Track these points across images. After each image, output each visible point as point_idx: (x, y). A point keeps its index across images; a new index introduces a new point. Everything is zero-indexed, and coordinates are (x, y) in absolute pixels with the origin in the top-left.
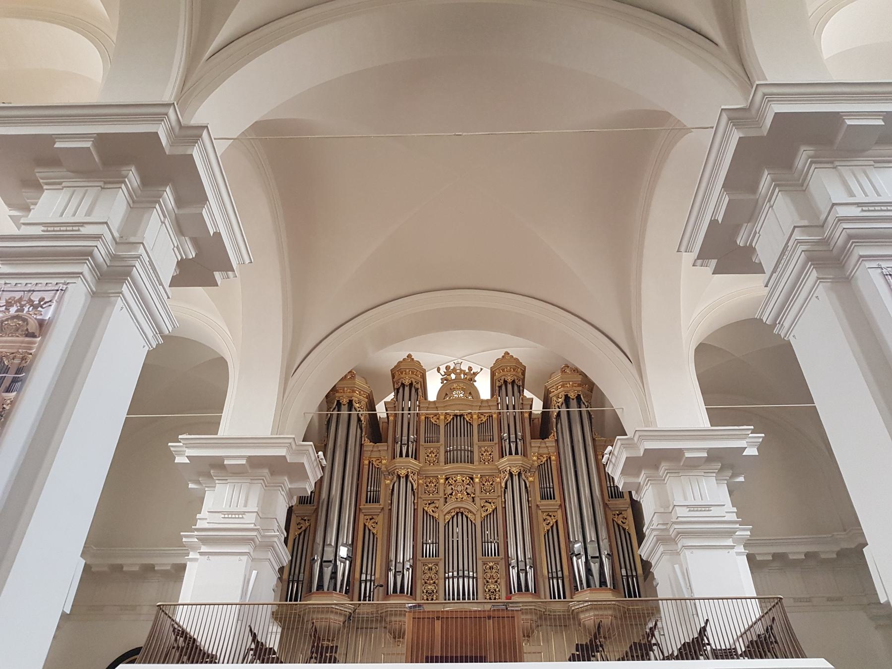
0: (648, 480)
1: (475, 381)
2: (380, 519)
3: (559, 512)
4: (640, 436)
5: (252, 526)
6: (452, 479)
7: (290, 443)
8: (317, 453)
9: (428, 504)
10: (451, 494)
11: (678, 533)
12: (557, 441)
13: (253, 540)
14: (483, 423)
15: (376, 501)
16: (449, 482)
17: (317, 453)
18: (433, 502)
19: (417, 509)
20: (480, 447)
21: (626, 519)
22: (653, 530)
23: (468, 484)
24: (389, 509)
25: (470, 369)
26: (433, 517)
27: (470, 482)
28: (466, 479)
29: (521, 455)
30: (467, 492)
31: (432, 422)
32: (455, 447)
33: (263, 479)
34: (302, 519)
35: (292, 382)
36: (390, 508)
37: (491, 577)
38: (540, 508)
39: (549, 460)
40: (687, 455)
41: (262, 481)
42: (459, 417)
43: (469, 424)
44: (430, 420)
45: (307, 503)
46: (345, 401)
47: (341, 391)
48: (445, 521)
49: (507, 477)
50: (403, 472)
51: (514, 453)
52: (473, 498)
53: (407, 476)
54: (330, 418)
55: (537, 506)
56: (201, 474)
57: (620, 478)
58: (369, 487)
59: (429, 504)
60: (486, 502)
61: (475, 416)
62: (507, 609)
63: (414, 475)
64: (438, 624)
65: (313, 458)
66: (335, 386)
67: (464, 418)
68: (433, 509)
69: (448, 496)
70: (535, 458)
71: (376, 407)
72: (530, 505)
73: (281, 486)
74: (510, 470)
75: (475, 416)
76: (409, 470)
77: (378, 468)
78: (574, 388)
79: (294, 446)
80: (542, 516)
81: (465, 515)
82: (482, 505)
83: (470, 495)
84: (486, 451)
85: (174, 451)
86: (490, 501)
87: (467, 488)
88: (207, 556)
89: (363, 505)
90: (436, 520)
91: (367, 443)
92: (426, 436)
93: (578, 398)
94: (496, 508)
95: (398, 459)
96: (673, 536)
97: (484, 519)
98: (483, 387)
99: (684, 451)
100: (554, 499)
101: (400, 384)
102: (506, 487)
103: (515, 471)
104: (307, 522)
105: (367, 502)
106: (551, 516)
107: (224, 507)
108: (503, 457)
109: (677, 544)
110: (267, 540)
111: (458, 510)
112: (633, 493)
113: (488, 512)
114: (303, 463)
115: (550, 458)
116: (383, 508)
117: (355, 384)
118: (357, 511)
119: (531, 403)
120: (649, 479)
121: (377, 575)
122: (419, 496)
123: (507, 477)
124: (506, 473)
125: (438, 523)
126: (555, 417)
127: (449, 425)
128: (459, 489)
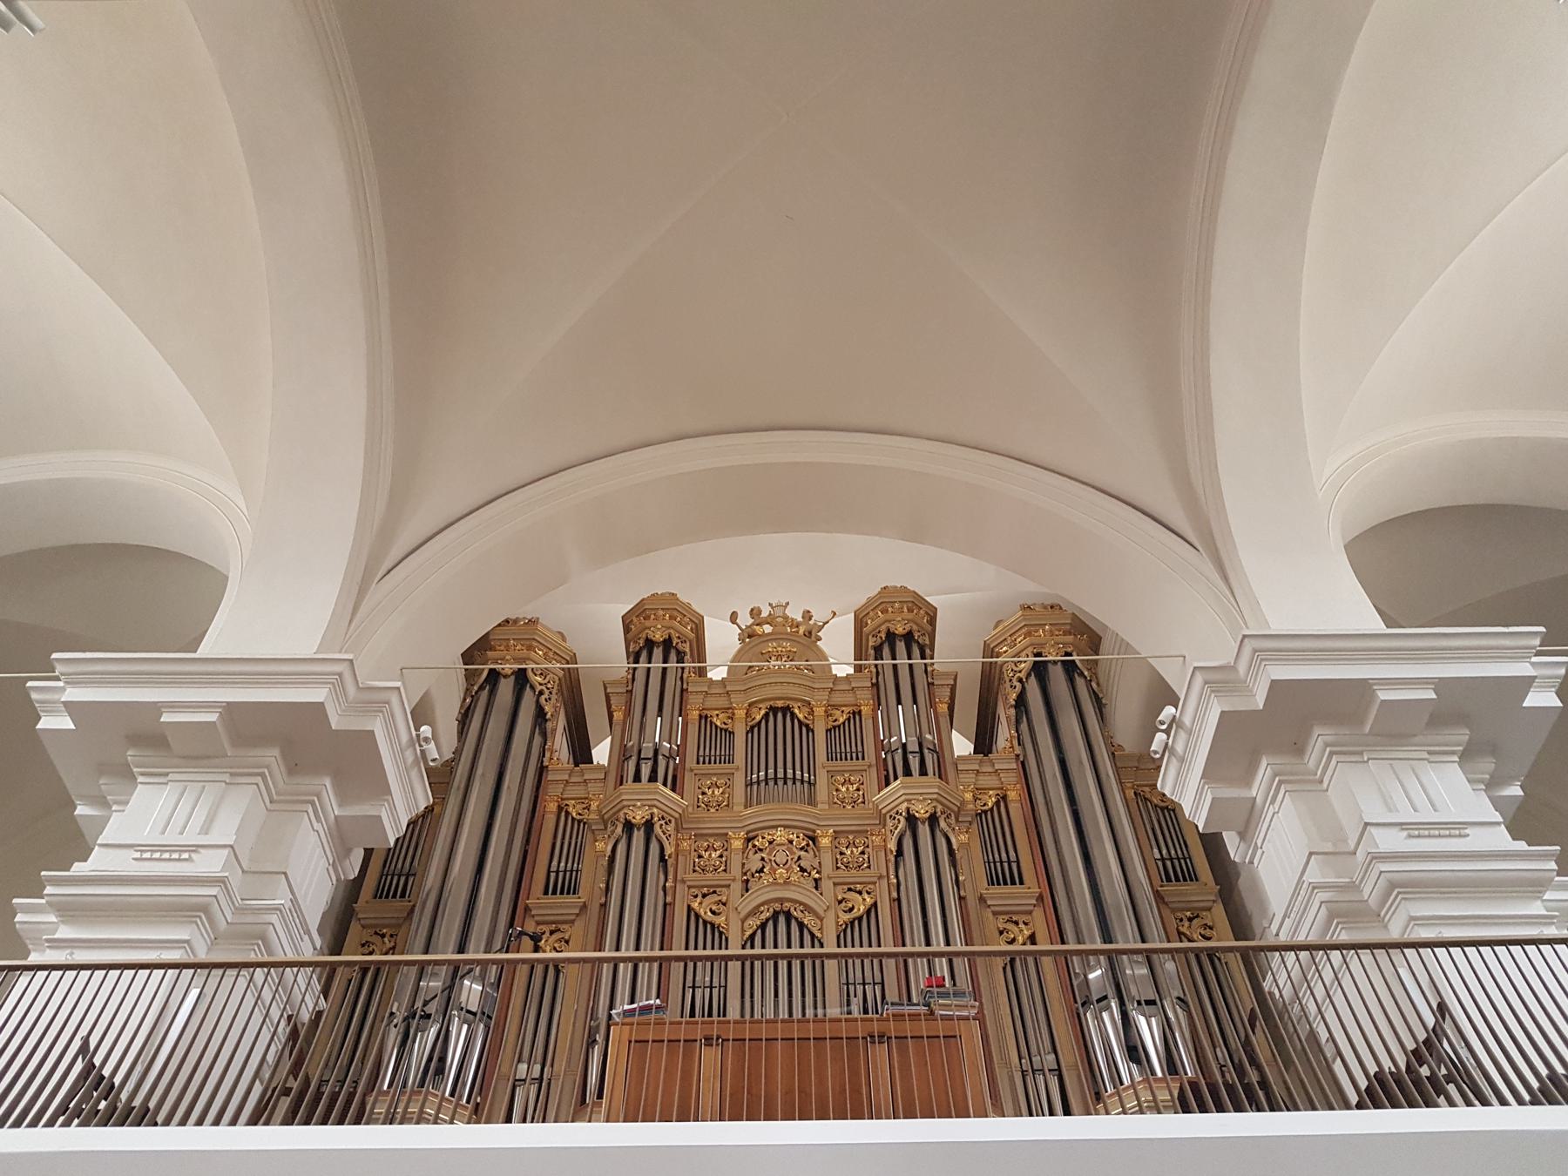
0: (1280, 782)
1: (820, 639)
4: (1255, 651)
6: (763, 838)
7: (340, 675)
8: (417, 729)
9: (700, 896)
10: (761, 871)
11: (1392, 885)
13: (205, 909)
14: (839, 726)
15: (571, 889)
16: (754, 846)
17: (417, 729)
18: (714, 892)
19: (673, 904)
21: (1211, 928)
22: (1315, 887)
23: (802, 849)
24: (601, 905)
25: (807, 615)
26: (713, 925)
27: (808, 845)
28: (798, 837)
29: (934, 775)
30: (799, 866)
31: (716, 726)
32: (771, 771)
33: (262, 775)
34: (376, 933)
35: (377, 593)
36: (603, 900)
38: (989, 903)
39: (1002, 804)
40: (1384, 695)
41: (259, 780)
42: (780, 715)
43: (804, 729)
44: (711, 722)
45: (394, 896)
47: (502, 648)
48: (743, 931)
49: (900, 826)
50: (639, 816)
52: (816, 880)
53: (649, 825)
54: (469, 708)
55: (982, 899)
56: (104, 769)
57: (1199, 793)
58: (555, 863)
59: (704, 896)
60: (850, 890)
61: (819, 711)
62: (932, 1013)
63: (666, 823)
65: (404, 738)
66: (488, 634)
67: (793, 715)
68: (714, 908)
69: (753, 876)
70: (969, 796)
71: (593, 751)
72: (962, 893)
73: (313, 803)
74: (908, 810)
75: (819, 711)
76: (655, 810)
77: (579, 822)
78: (1061, 639)
79: (351, 690)
81: (796, 919)
82: (840, 898)
83: (810, 874)
85: (38, 702)
86: (859, 887)
87: (799, 858)
88: (68, 951)
89: (536, 898)
90: (721, 933)
92: (701, 753)
94: (875, 905)
95: (629, 784)
96: (1373, 902)
97: (845, 931)
98: (841, 660)
99: (1375, 687)
100: (1021, 883)
101: (642, 643)
102: (900, 852)
103: (921, 811)
104: (386, 940)
105: (546, 893)
106: (1016, 923)
107: (148, 835)
108: (888, 784)
109: (1386, 927)
110: (249, 919)
111: (777, 906)
112: (1231, 841)
113: (855, 913)
114: (373, 731)
115: (1004, 798)
119: (952, 683)
120: (1282, 779)
122: (679, 878)
123: (900, 826)
124: (897, 817)
125: (727, 939)
126: (1014, 703)
127: (756, 730)
128: (781, 858)
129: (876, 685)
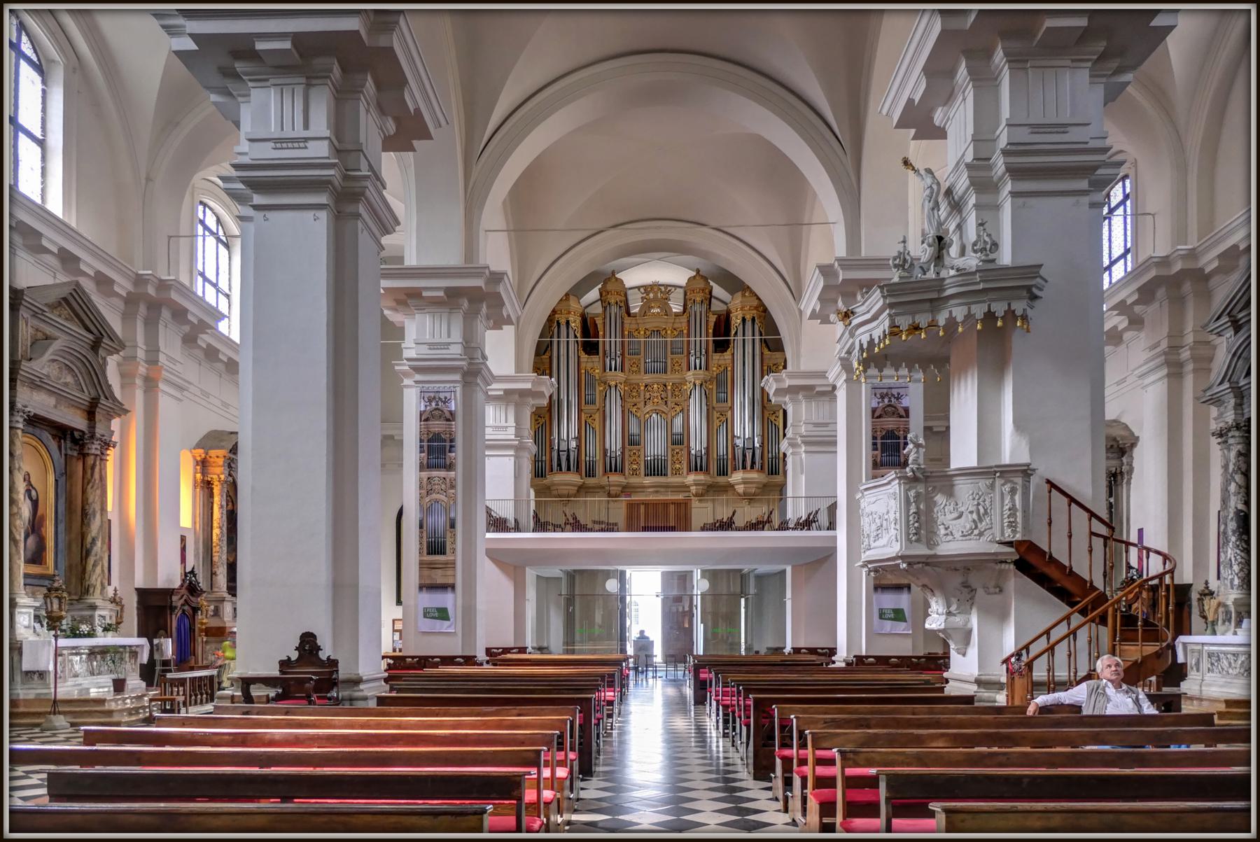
2: (597, 416)
3: (730, 412)
5: (513, 437)
12: (733, 354)
15: (593, 403)
20: (672, 359)
37: (678, 459)
40: (818, 389)
46: (563, 321)
51: (698, 368)
53: (616, 386)
55: (713, 408)
64: (642, 507)
70: (714, 369)
80: (716, 415)
84: (677, 362)
91: (583, 355)
93: (753, 320)
116: (598, 409)
117: (570, 306)
118: (580, 411)
121: (598, 458)
128: (655, 394)
129: (689, 321)
